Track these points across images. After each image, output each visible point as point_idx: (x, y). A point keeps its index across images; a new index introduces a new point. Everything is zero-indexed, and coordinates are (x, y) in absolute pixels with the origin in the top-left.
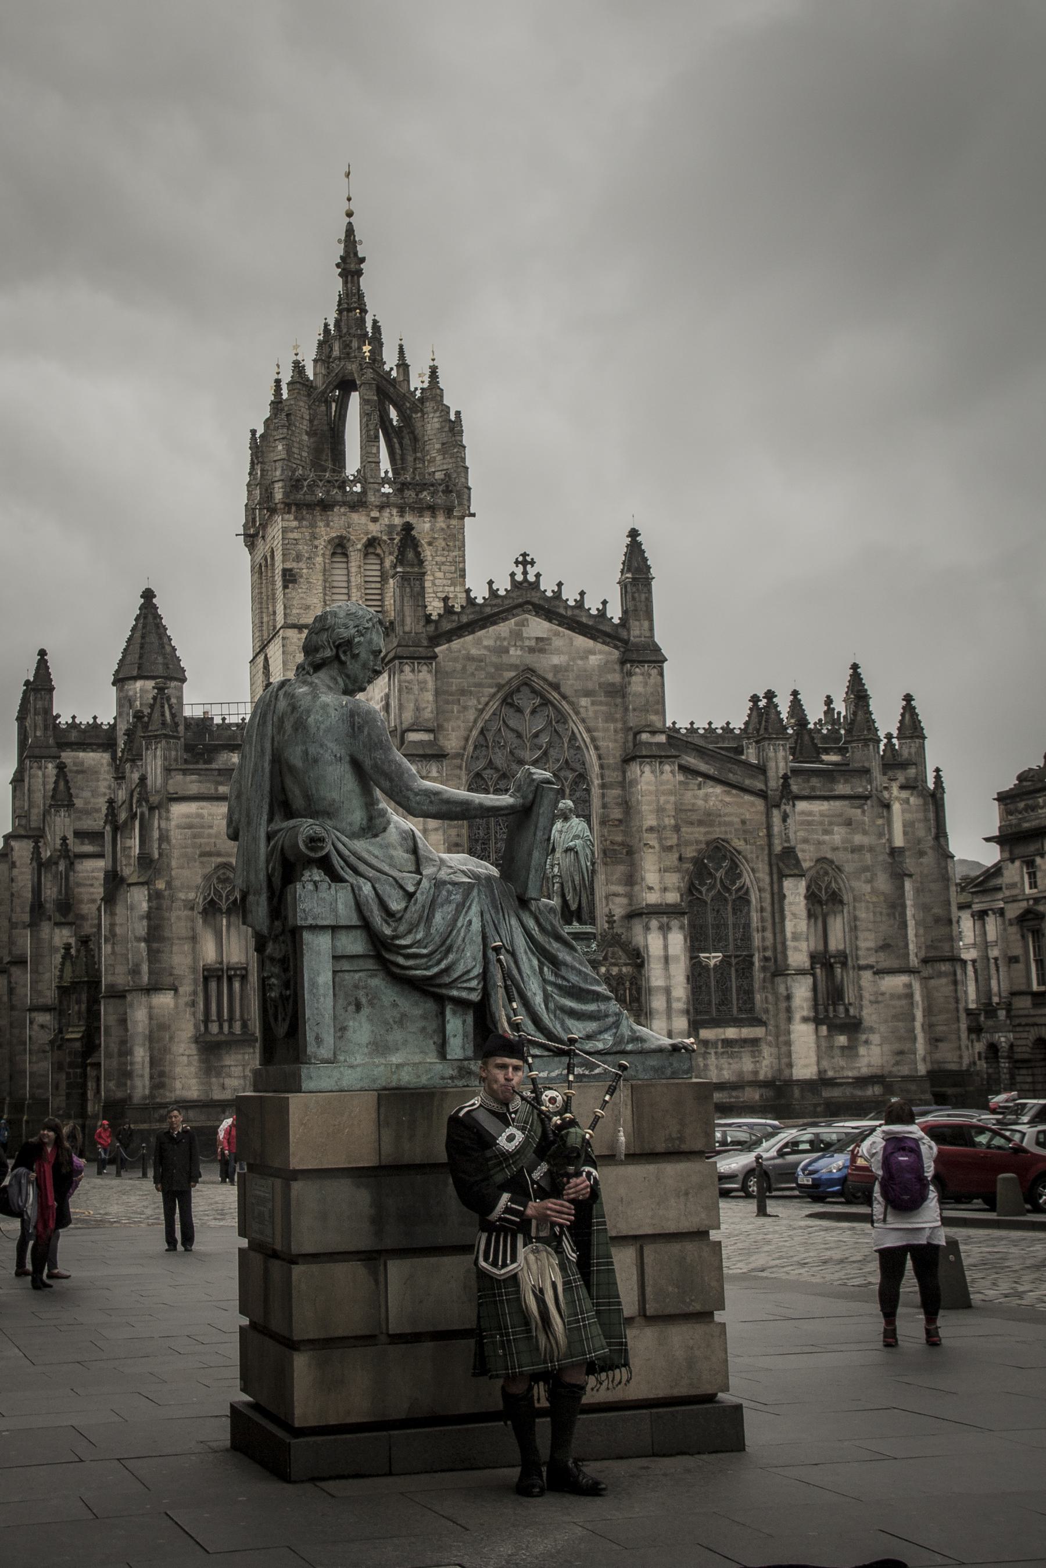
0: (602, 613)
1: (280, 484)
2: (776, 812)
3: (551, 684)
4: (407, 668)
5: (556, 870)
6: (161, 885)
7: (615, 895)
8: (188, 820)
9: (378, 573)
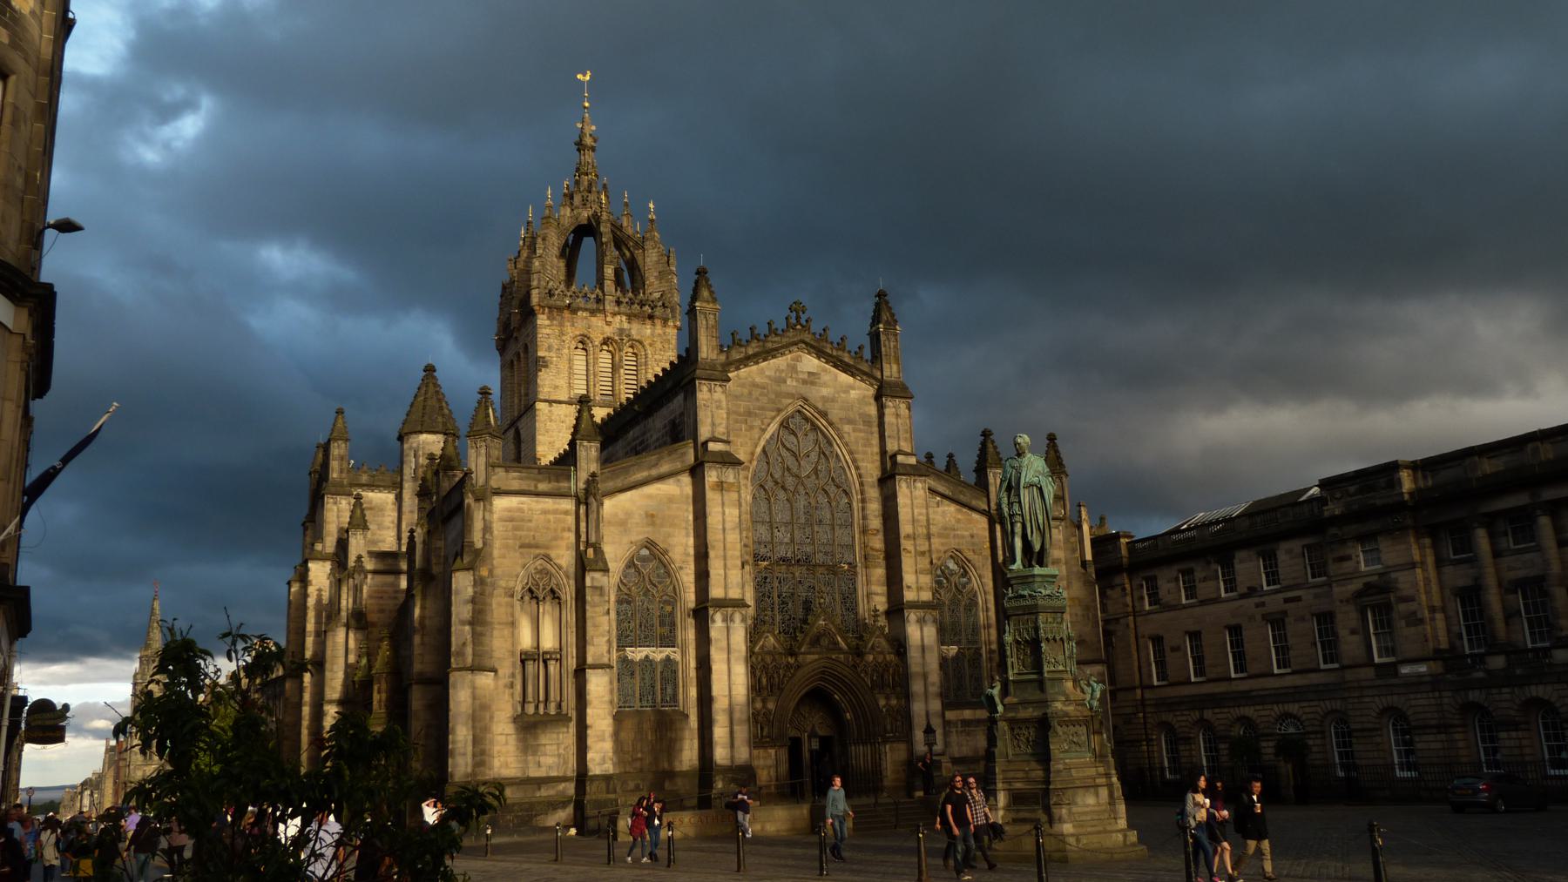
1: (536, 291)
3: (820, 412)
4: (705, 389)
5: (1016, 507)
6: (484, 572)
7: (875, 594)
8: (510, 514)
9: (610, 366)
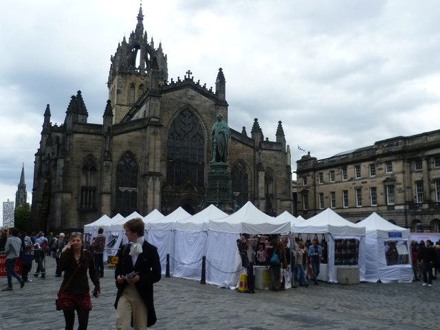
0: (211, 90)
2: (257, 153)
4: (152, 99)
